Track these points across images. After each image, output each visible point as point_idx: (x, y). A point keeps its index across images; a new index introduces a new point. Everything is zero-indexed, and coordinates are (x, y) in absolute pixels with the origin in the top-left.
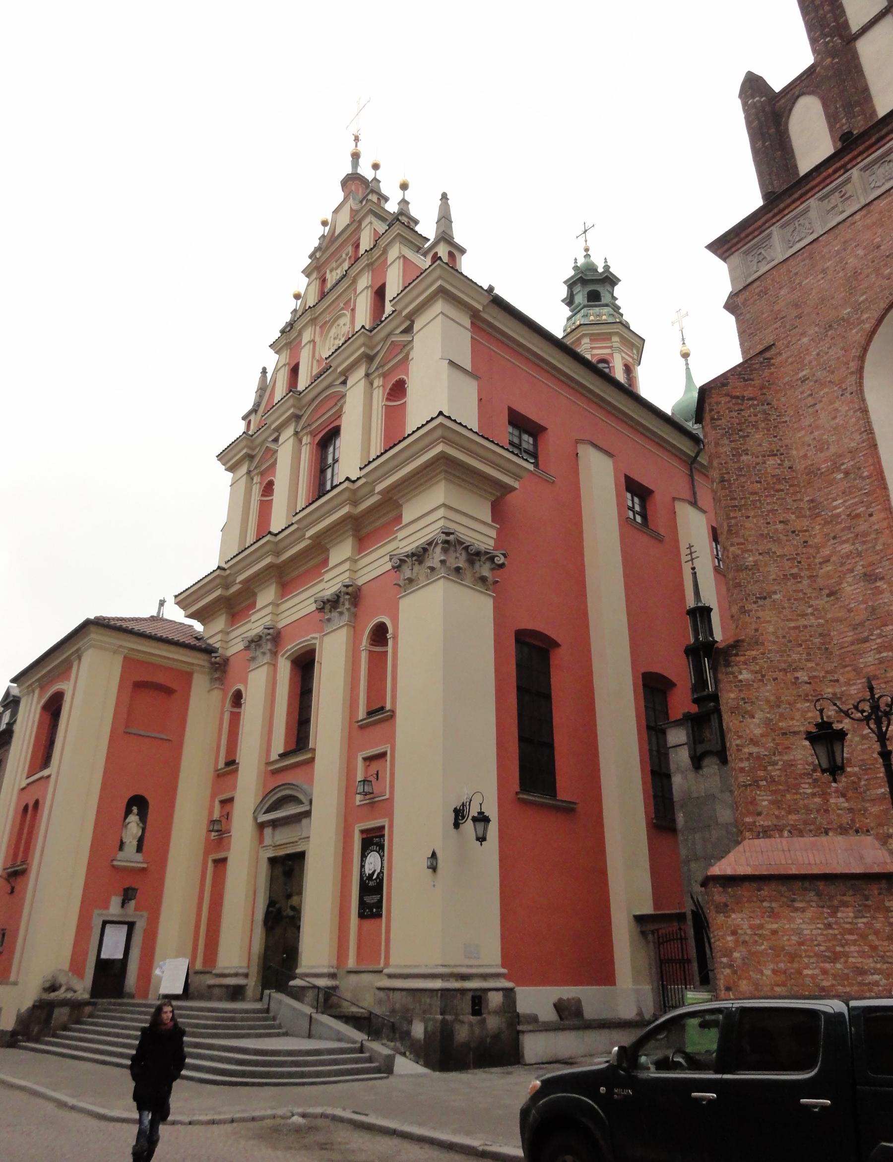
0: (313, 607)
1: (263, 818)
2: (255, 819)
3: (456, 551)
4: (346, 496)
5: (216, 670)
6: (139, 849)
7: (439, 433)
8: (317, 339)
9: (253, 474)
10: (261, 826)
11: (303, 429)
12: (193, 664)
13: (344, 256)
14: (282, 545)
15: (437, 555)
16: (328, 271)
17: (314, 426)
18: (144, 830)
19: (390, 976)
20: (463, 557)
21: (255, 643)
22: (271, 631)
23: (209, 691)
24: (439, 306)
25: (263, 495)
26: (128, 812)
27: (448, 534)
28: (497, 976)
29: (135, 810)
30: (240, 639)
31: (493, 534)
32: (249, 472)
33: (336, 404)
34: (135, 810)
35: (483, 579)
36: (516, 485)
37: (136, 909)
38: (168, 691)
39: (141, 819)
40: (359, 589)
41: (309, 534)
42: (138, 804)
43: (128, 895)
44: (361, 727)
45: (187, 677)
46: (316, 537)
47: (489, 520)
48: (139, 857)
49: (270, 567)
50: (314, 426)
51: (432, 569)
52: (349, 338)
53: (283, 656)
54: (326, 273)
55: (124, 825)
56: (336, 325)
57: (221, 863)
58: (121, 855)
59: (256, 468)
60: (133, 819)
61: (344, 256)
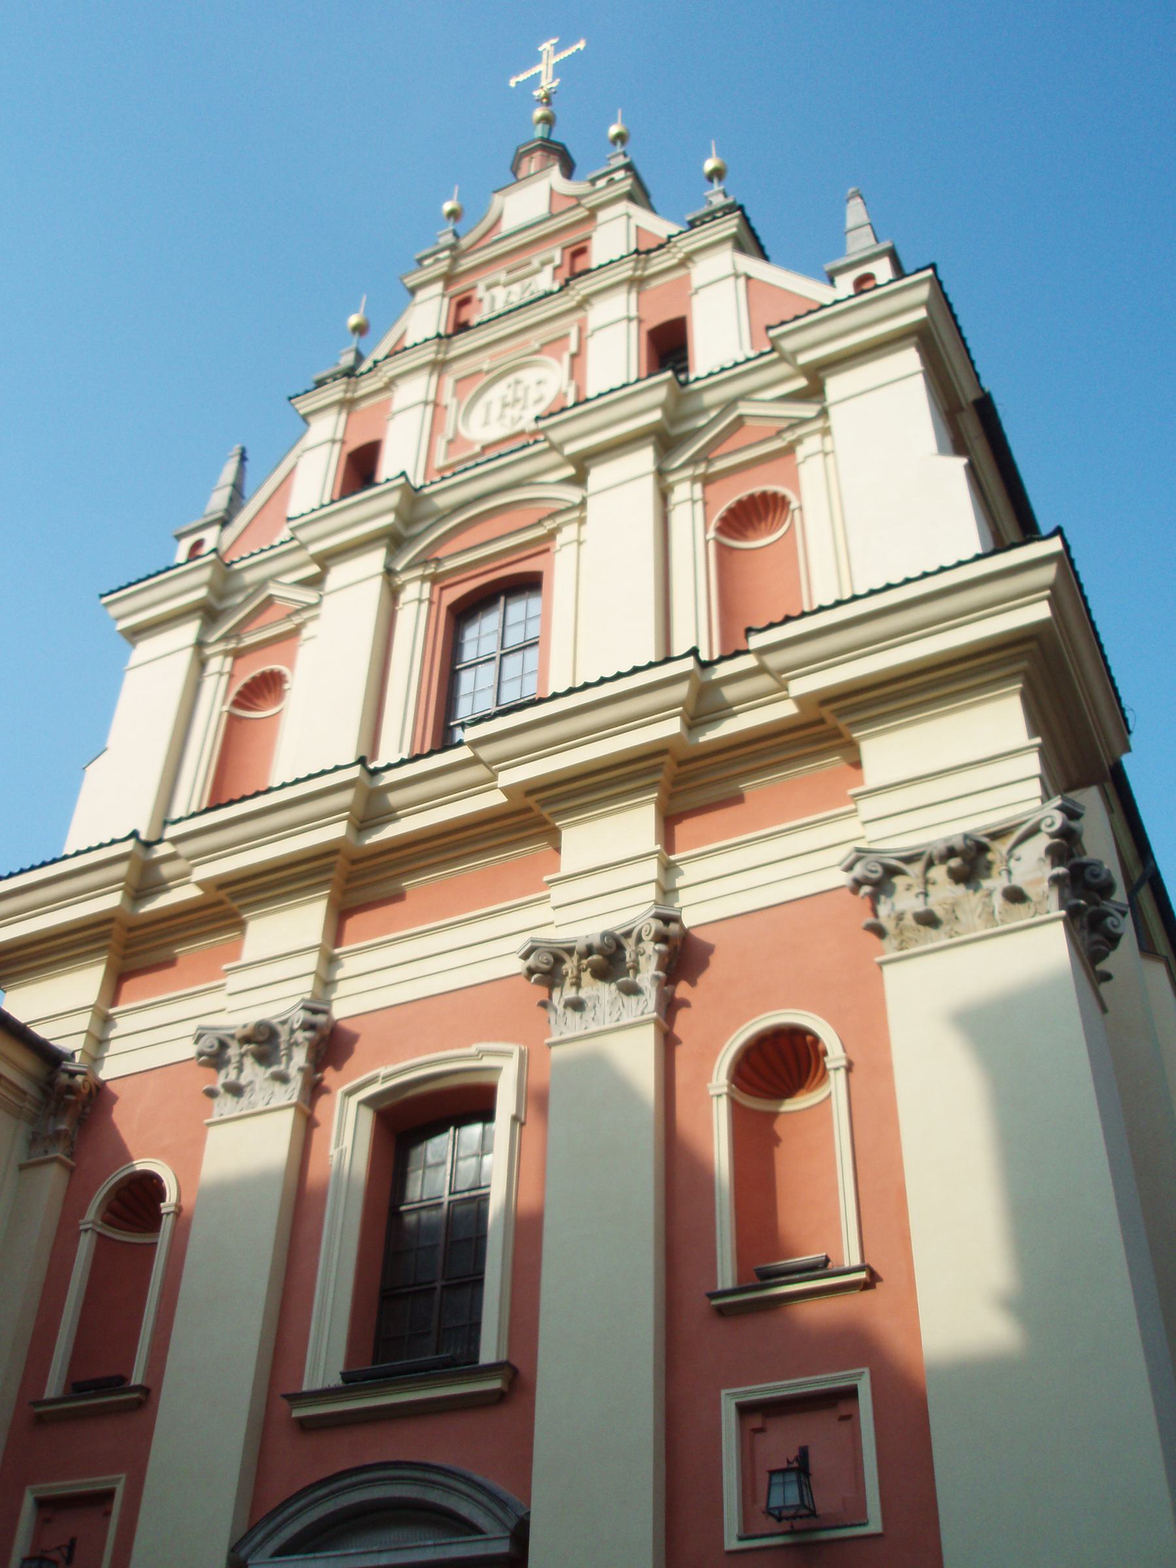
8: (448, 398)
9: (208, 651)
11: (409, 567)
13: (536, 264)
16: (481, 286)
22: (321, 1019)
23: (22, 1167)
25: (236, 704)
30: (191, 1028)
33: (539, 523)
44: (722, 1312)
46: (532, 789)
51: (1015, 896)
52: (564, 409)
53: (350, 1093)
54: (474, 288)
56: (510, 379)
59: (225, 638)
61: (536, 264)
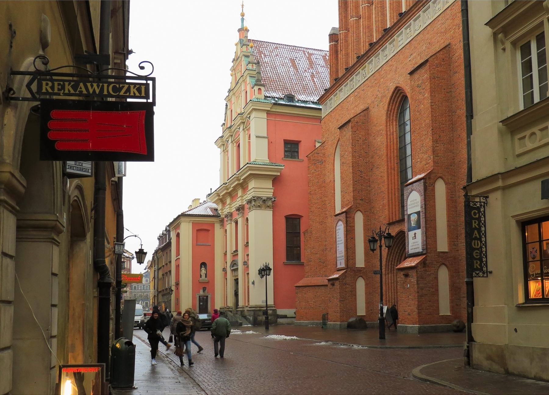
0: (234, 209)
1: (232, 269)
2: (230, 268)
3: (258, 201)
4: (236, 179)
5: (221, 222)
6: (206, 277)
7: (248, 169)
9: (225, 151)
10: (232, 270)
12: (214, 221)
14: (228, 187)
15: (253, 203)
17: (236, 140)
18: (206, 271)
19: (250, 307)
20: (261, 203)
21: (226, 216)
24: (253, 115)
26: (201, 267)
27: (254, 197)
28: (272, 307)
29: (203, 266)
31: (272, 191)
32: (224, 151)
34: (203, 266)
35: (268, 206)
36: (279, 174)
37: (207, 293)
38: (208, 230)
39: (205, 269)
40: (244, 206)
41: (232, 187)
42: (203, 264)
43: (204, 289)
45: (213, 225)
47: (271, 187)
48: (206, 279)
49: (226, 193)
50: (236, 140)
55: (201, 271)
57: (226, 279)
58: (201, 279)
60: (203, 269)
